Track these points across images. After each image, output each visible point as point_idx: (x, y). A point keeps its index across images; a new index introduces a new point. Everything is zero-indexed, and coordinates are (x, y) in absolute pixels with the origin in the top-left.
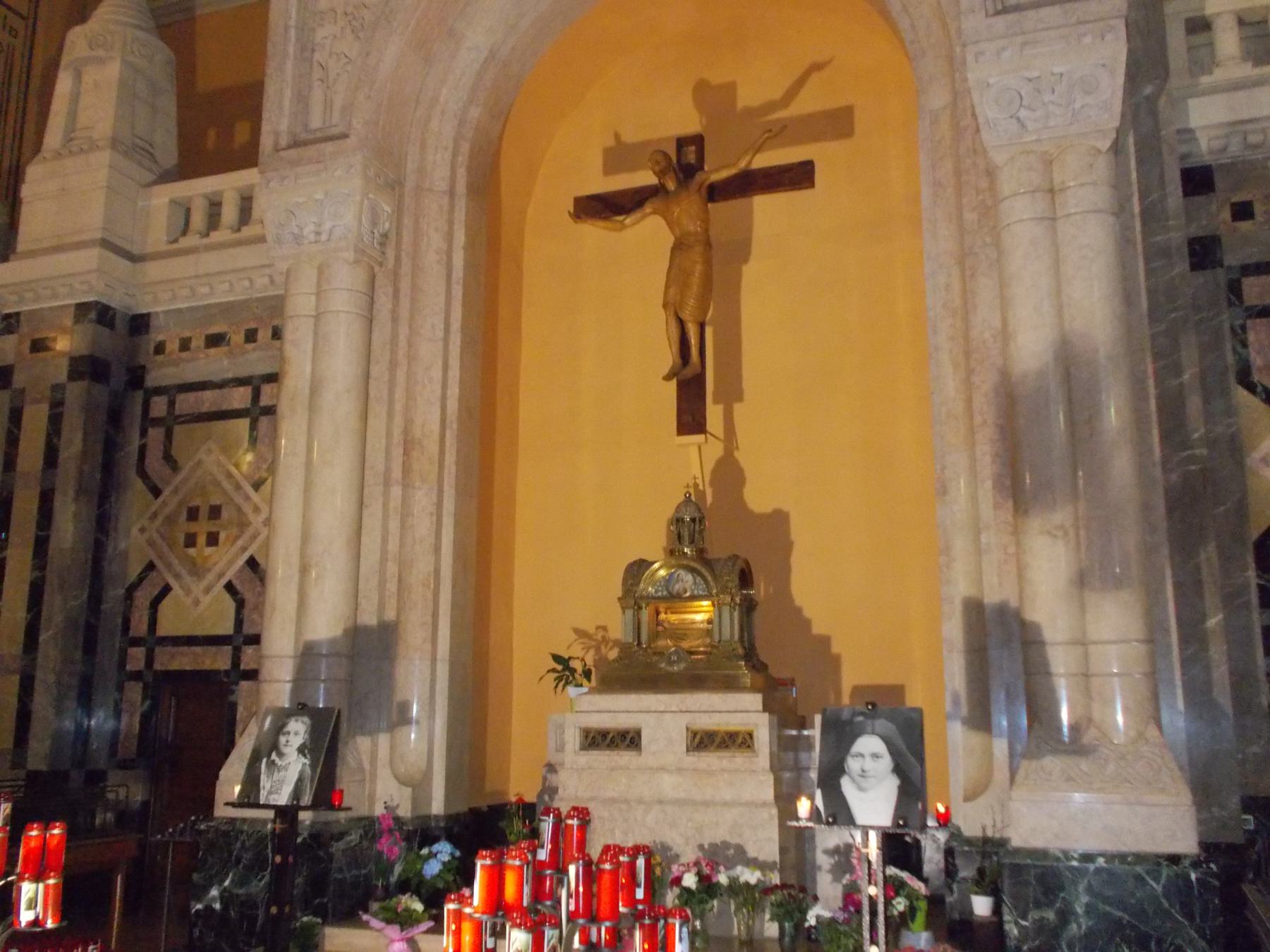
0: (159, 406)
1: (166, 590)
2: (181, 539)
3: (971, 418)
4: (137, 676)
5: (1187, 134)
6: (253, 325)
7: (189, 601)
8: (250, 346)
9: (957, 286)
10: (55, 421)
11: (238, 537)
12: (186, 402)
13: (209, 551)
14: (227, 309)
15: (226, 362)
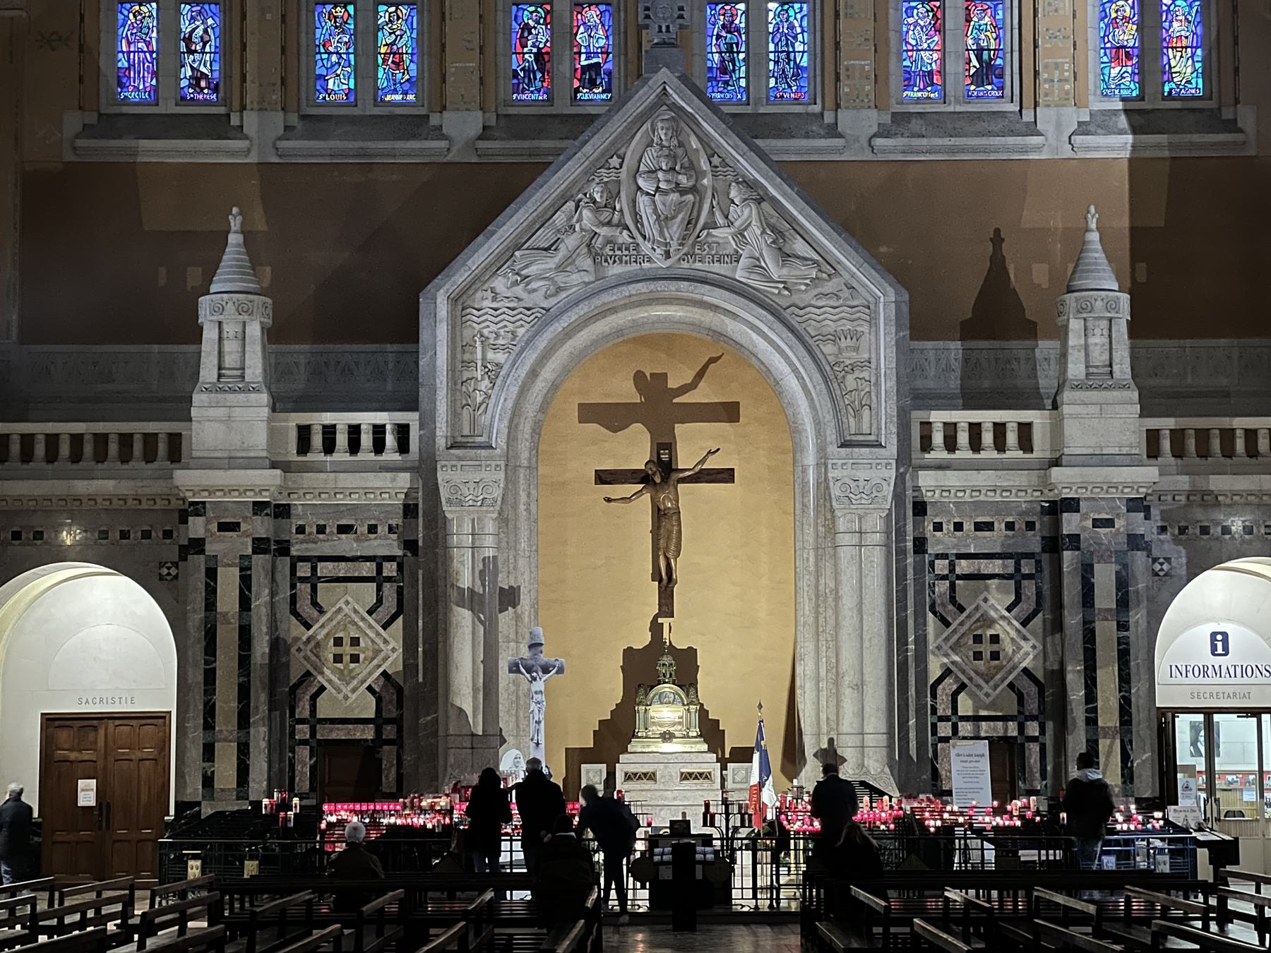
0: (304, 570)
1: (322, 689)
2: (331, 657)
3: (817, 627)
4: (304, 742)
5: (917, 489)
6: (373, 522)
7: (340, 696)
8: (372, 536)
9: (812, 560)
10: (246, 581)
11: (373, 659)
12: (325, 569)
13: (352, 665)
14: (353, 509)
15: (355, 545)
